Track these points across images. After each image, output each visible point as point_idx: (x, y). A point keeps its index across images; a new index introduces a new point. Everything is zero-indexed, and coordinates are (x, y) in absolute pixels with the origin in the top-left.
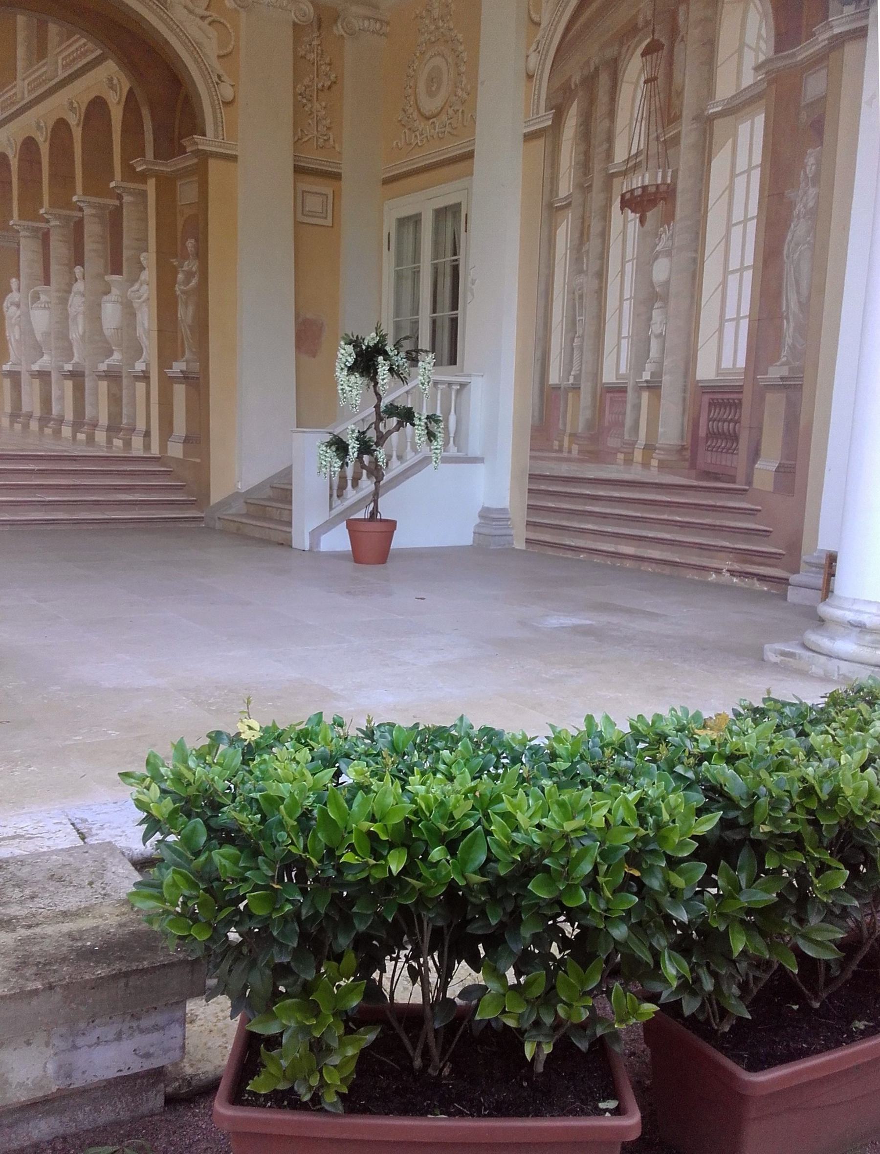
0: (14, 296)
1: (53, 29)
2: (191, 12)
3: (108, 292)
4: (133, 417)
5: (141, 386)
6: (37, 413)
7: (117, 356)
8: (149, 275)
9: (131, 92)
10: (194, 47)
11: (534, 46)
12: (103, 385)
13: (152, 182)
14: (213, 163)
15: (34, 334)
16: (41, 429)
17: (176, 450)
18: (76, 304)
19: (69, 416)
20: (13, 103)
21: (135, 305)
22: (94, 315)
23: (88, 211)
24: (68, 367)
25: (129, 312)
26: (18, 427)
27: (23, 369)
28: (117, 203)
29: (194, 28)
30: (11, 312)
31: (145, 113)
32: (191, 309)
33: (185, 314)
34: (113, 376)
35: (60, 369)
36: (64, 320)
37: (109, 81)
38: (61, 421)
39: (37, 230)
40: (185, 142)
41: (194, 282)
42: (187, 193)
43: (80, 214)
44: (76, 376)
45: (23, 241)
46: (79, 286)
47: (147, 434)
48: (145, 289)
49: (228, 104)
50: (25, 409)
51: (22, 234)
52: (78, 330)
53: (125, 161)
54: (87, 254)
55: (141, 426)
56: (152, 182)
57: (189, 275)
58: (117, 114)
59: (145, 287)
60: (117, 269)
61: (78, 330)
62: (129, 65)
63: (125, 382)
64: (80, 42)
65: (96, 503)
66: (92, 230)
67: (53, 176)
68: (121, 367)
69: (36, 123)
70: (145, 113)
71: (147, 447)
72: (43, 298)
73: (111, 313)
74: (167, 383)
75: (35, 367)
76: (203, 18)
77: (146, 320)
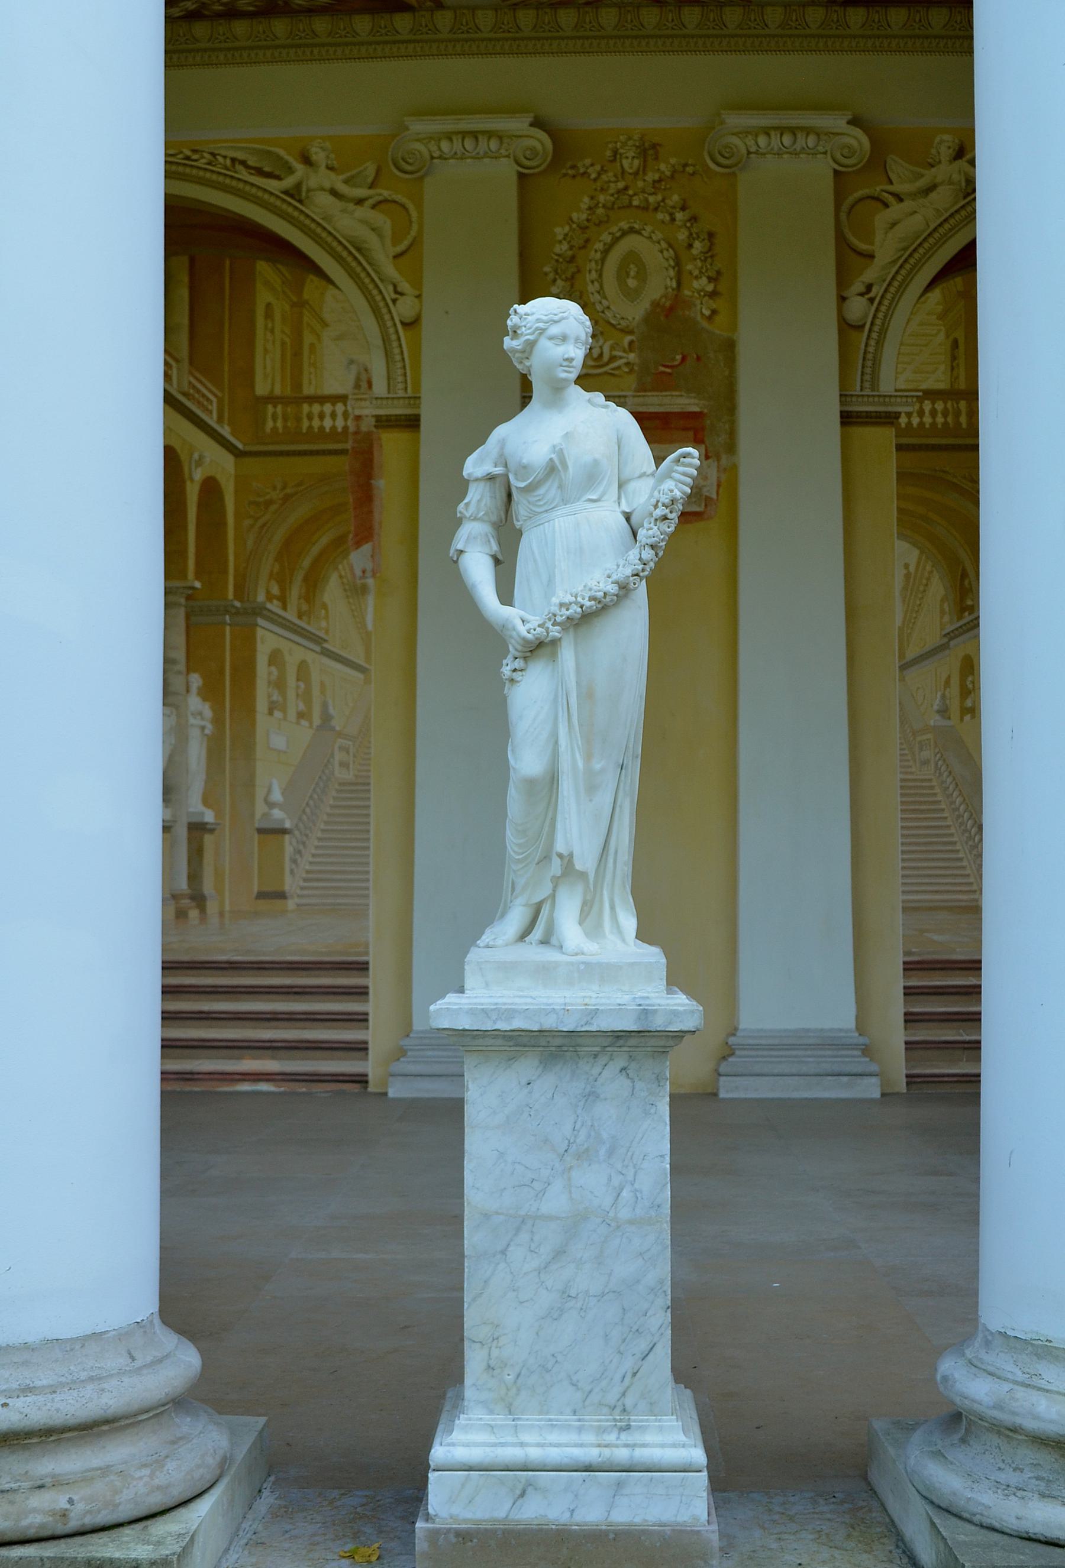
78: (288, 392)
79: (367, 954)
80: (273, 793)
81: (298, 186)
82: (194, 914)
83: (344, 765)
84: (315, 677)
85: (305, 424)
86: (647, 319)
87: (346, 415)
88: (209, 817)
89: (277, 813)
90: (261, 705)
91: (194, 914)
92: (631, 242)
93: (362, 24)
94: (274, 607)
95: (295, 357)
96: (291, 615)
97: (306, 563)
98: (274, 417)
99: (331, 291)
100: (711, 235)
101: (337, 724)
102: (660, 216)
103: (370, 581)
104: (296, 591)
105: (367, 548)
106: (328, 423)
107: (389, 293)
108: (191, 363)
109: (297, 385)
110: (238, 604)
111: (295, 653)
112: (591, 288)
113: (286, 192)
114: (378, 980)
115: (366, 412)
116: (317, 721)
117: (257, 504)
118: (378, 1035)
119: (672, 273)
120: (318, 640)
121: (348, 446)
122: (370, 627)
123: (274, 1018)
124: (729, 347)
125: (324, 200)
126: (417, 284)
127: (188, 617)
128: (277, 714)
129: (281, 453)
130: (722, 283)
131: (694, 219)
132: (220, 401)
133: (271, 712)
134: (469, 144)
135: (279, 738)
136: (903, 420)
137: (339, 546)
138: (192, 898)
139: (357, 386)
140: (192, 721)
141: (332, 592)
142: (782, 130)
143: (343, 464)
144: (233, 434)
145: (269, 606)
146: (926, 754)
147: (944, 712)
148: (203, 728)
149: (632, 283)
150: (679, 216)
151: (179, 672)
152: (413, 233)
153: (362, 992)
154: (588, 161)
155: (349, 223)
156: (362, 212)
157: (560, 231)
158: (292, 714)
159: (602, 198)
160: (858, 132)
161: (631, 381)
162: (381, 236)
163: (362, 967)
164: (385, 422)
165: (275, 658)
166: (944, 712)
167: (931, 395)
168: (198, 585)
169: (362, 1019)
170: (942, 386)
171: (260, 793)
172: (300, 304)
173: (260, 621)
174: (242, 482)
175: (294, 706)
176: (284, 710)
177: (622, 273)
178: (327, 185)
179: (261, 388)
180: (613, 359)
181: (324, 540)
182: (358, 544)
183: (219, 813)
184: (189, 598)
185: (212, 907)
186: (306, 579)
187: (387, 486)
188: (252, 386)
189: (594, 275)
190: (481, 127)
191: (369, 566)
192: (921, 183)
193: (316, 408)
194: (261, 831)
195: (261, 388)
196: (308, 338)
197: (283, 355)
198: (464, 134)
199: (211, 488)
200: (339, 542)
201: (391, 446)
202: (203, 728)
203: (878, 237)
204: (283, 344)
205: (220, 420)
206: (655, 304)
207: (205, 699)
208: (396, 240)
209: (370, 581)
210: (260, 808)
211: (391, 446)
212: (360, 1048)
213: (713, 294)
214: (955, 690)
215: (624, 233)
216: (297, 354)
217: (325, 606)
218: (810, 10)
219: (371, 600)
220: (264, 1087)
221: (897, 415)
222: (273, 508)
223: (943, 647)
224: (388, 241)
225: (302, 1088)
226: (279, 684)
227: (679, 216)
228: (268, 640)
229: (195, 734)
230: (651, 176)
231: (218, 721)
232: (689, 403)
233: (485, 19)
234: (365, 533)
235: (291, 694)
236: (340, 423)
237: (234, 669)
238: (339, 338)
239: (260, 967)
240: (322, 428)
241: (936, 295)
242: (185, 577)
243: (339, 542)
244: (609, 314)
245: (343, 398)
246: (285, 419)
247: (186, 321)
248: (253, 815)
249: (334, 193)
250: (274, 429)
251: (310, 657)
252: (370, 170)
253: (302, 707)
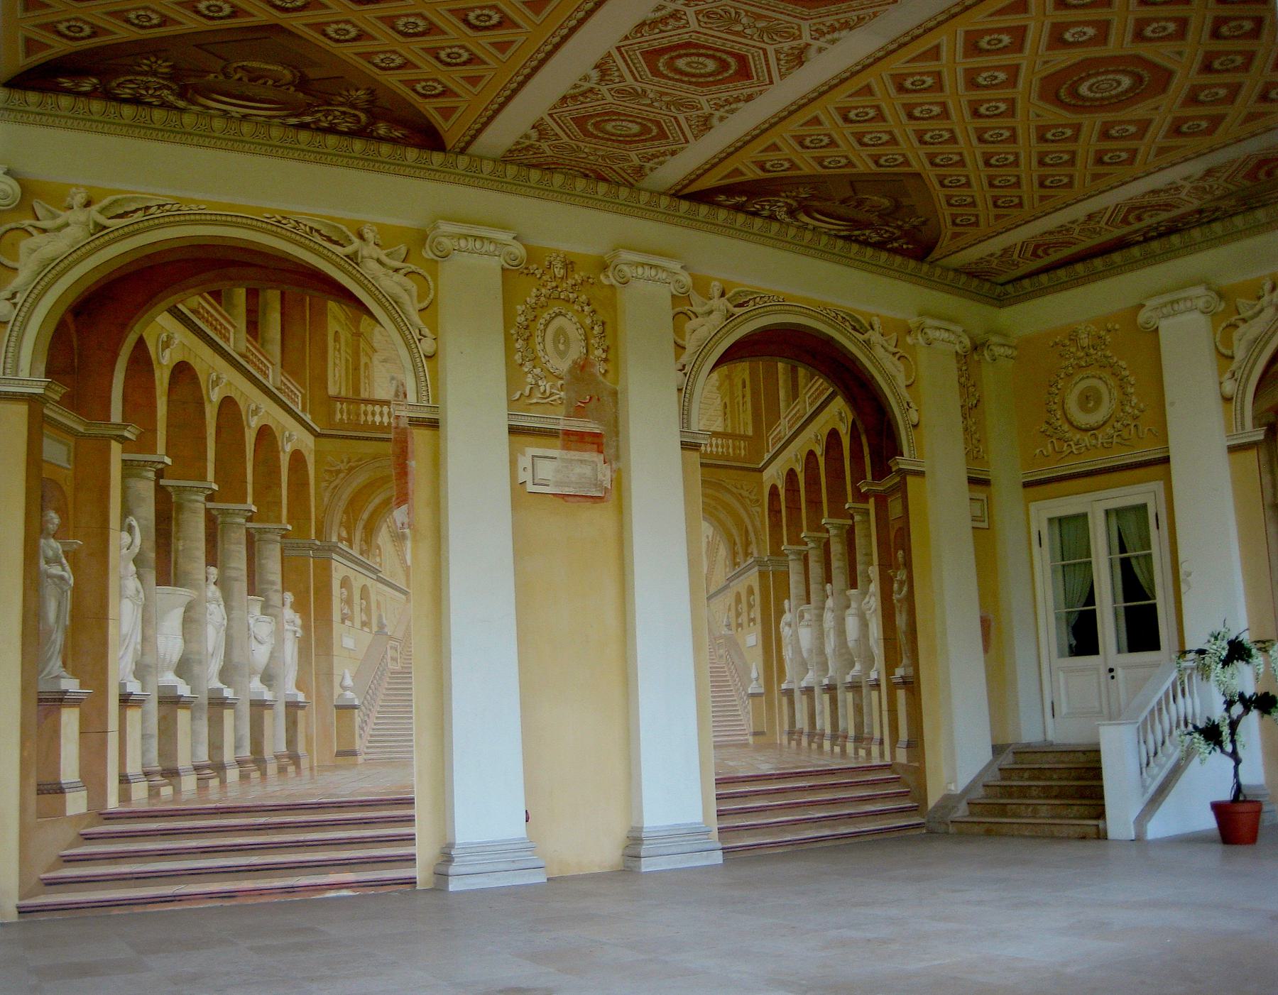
0: (787, 617)
1: (802, 372)
2: (886, 350)
3: (848, 607)
4: (871, 726)
5: (875, 694)
6: (806, 730)
7: (858, 667)
8: (874, 587)
9: (854, 423)
10: (890, 379)
11: (1228, 375)
12: (850, 696)
13: (872, 500)
14: (909, 479)
15: (801, 652)
16: (809, 745)
17: (902, 756)
18: (828, 617)
19: (828, 731)
20: (780, 439)
21: (868, 617)
23: (833, 532)
24: (826, 681)
25: (864, 625)
26: (794, 743)
27: (795, 686)
28: (850, 522)
29: (890, 363)
30: (786, 631)
31: (864, 439)
32: (904, 616)
33: (901, 620)
34: (855, 687)
35: (820, 683)
36: (821, 636)
38: (823, 735)
39: (799, 553)
40: (891, 463)
41: (905, 589)
42: (895, 508)
43: (826, 535)
44: (831, 689)
45: (791, 565)
46: (830, 603)
47: (881, 742)
48: (873, 602)
49: (915, 426)
50: (798, 726)
51: (791, 557)
53: (854, 483)
54: (835, 572)
55: (877, 735)
56: (872, 500)
57: (901, 583)
58: (846, 442)
59: (873, 599)
60: (853, 585)
62: (851, 400)
63: (864, 691)
64: (820, 382)
65: (850, 816)
66: (836, 548)
67: (809, 501)
68: (859, 677)
69: (792, 458)
70: (864, 439)
71: (882, 755)
72: (806, 615)
73: (852, 624)
74: (892, 688)
75: (804, 684)
76: (894, 354)
78: (350, 395)
79: (412, 792)
80: (346, 680)
81: (356, 253)
82: (291, 769)
83: (393, 659)
84: (373, 597)
85: (363, 418)
86: (571, 371)
87: (389, 414)
88: (301, 697)
89: (349, 694)
90: (336, 616)
91: (291, 769)
92: (559, 321)
93: (412, 154)
94: (344, 546)
95: (355, 370)
96: (355, 552)
97: (365, 516)
98: (342, 413)
99: (378, 328)
100: (603, 323)
101: (388, 630)
102: (576, 307)
103: (407, 531)
104: (358, 535)
105: (404, 507)
106: (378, 419)
107: (416, 336)
108: (282, 366)
109: (357, 390)
110: (318, 543)
111: (360, 580)
112: (539, 347)
113: (347, 256)
114: (422, 812)
115: (403, 414)
116: (375, 628)
117: (331, 472)
118: (425, 850)
119: (583, 344)
120: (375, 571)
121: (391, 436)
122: (409, 563)
123: (351, 842)
124: (615, 393)
125: (373, 265)
126: (434, 330)
127: (282, 551)
128: (348, 623)
129: (347, 437)
130: (611, 354)
131: (594, 311)
132: (304, 396)
133: (343, 622)
134: (478, 244)
135: (348, 638)
136: (703, 448)
137: (386, 505)
138: (290, 757)
139: (397, 395)
140: (287, 627)
141: (383, 538)
142: (651, 266)
143: (389, 448)
144: (313, 420)
145: (340, 545)
146: (721, 651)
147: (728, 626)
148: (295, 632)
149: (561, 347)
150: (586, 308)
151: (276, 591)
152: (431, 296)
153: (410, 820)
154: (535, 266)
155: (391, 283)
156: (398, 277)
157: (520, 308)
158: (358, 624)
159: (543, 291)
160: (685, 274)
161: (562, 410)
162: (410, 295)
163: (410, 802)
164: (416, 422)
165: (345, 583)
166: (728, 626)
167: (715, 434)
168: (289, 527)
169: (410, 839)
170: (720, 430)
171: (337, 680)
172: (358, 335)
173: (334, 556)
174: (319, 454)
175: (359, 617)
176: (352, 620)
177: (556, 341)
178: (375, 256)
179: (332, 391)
180: (552, 394)
181: (377, 501)
182: (399, 505)
183: (308, 695)
184: (283, 537)
185: (304, 763)
186: (365, 527)
187: (418, 465)
188: (326, 388)
189: (540, 339)
190: (484, 234)
191: (406, 520)
192: (706, 308)
193: (370, 408)
194: (338, 707)
195: (332, 391)
196: (363, 360)
197: (347, 367)
198: (476, 238)
199: (297, 457)
200: (386, 502)
201: (420, 438)
202: (295, 632)
203: (687, 337)
204: (347, 360)
205: (304, 410)
206: (575, 363)
207: (296, 611)
208: (421, 298)
209: (407, 531)
210: (337, 691)
211: (420, 438)
212: (410, 859)
213: (606, 360)
214: (733, 612)
215: (557, 315)
216: (356, 368)
217: (379, 547)
218: (663, 198)
219: (409, 544)
220: (345, 893)
221: (699, 445)
222: (342, 475)
223: (726, 587)
224: (415, 299)
225: (371, 891)
226: (349, 601)
227: (586, 308)
228: (340, 569)
229: (289, 637)
230: (571, 281)
231: (305, 627)
232: (590, 426)
233: (488, 166)
234: (403, 497)
235: (357, 609)
236: (386, 420)
237: (317, 590)
238: (385, 361)
239: (340, 806)
240: (374, 422)
241: (715, 375)
242: (279, 520)
243: (386, 502)
244: (549, 365)
245: (387, 403)
246: (349, 413)
247: (279, 336)
248: (332, 695)
249: (379, 261)
250: (342, 420)
251: (369, 582)
252: (403, 250)
253: (364, 618)
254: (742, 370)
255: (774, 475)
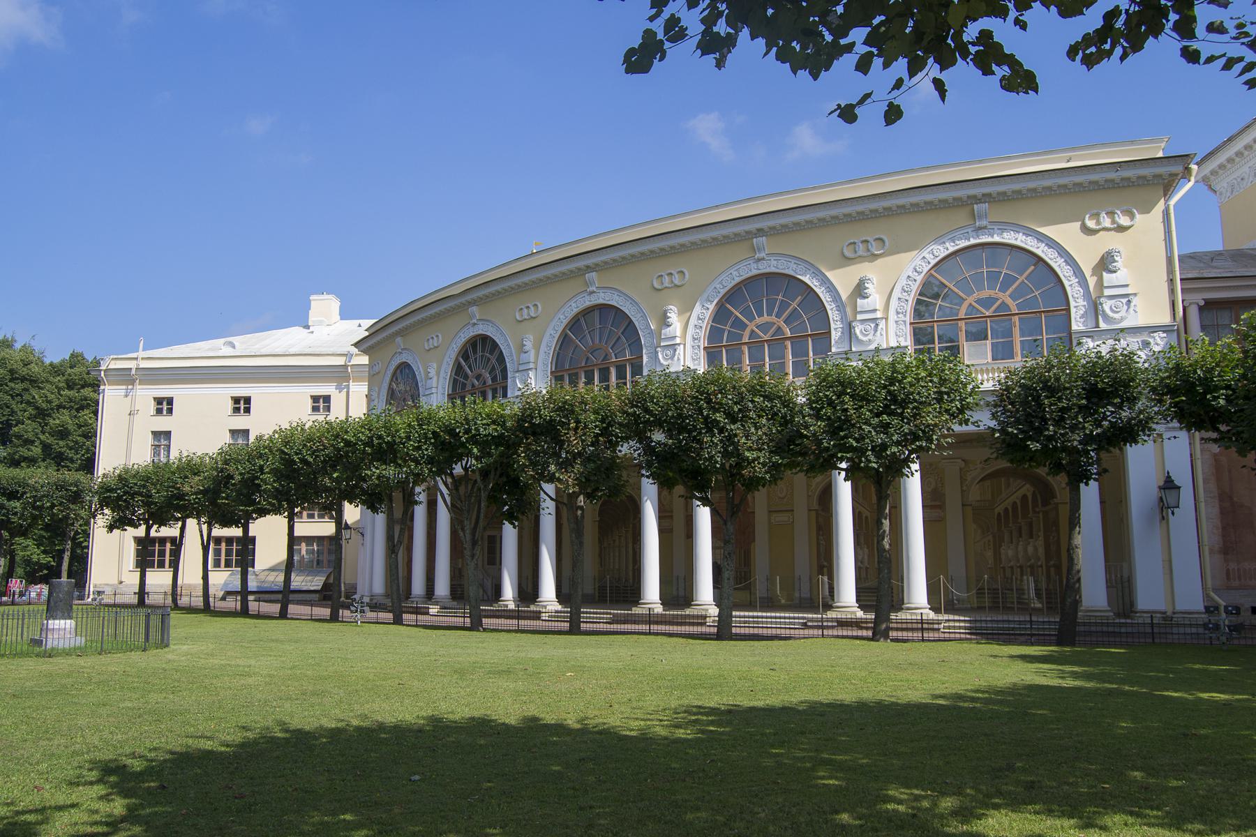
18: (1020, 548)
22: (1025, 550)
25: (1036, 549)
37: (1027, 489)
44: (1021, 567)
48: (1040, 542)
52: (1021, 555)
61: (1021, 555)
73: (1030, 549)
77: (1041, 551)
254: (988, 483)
255: (999, 509)
